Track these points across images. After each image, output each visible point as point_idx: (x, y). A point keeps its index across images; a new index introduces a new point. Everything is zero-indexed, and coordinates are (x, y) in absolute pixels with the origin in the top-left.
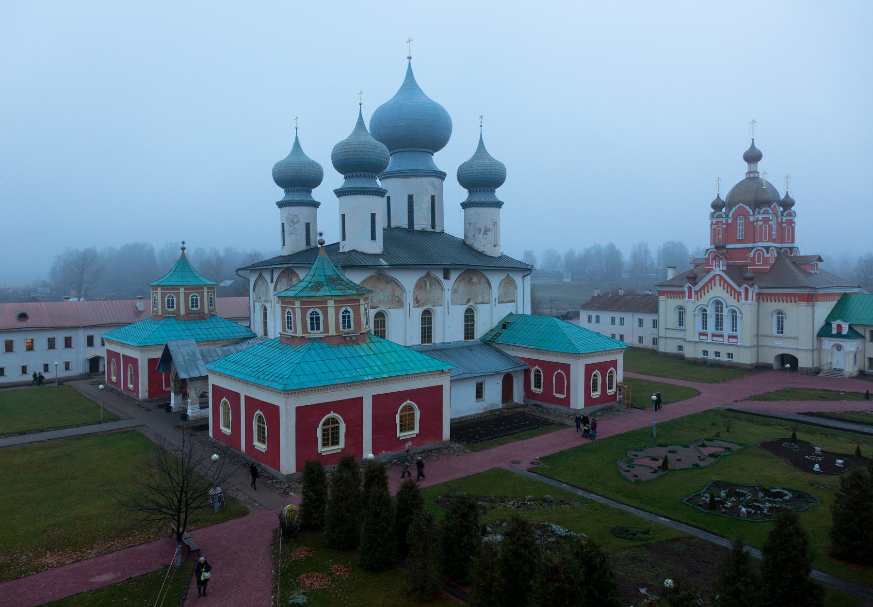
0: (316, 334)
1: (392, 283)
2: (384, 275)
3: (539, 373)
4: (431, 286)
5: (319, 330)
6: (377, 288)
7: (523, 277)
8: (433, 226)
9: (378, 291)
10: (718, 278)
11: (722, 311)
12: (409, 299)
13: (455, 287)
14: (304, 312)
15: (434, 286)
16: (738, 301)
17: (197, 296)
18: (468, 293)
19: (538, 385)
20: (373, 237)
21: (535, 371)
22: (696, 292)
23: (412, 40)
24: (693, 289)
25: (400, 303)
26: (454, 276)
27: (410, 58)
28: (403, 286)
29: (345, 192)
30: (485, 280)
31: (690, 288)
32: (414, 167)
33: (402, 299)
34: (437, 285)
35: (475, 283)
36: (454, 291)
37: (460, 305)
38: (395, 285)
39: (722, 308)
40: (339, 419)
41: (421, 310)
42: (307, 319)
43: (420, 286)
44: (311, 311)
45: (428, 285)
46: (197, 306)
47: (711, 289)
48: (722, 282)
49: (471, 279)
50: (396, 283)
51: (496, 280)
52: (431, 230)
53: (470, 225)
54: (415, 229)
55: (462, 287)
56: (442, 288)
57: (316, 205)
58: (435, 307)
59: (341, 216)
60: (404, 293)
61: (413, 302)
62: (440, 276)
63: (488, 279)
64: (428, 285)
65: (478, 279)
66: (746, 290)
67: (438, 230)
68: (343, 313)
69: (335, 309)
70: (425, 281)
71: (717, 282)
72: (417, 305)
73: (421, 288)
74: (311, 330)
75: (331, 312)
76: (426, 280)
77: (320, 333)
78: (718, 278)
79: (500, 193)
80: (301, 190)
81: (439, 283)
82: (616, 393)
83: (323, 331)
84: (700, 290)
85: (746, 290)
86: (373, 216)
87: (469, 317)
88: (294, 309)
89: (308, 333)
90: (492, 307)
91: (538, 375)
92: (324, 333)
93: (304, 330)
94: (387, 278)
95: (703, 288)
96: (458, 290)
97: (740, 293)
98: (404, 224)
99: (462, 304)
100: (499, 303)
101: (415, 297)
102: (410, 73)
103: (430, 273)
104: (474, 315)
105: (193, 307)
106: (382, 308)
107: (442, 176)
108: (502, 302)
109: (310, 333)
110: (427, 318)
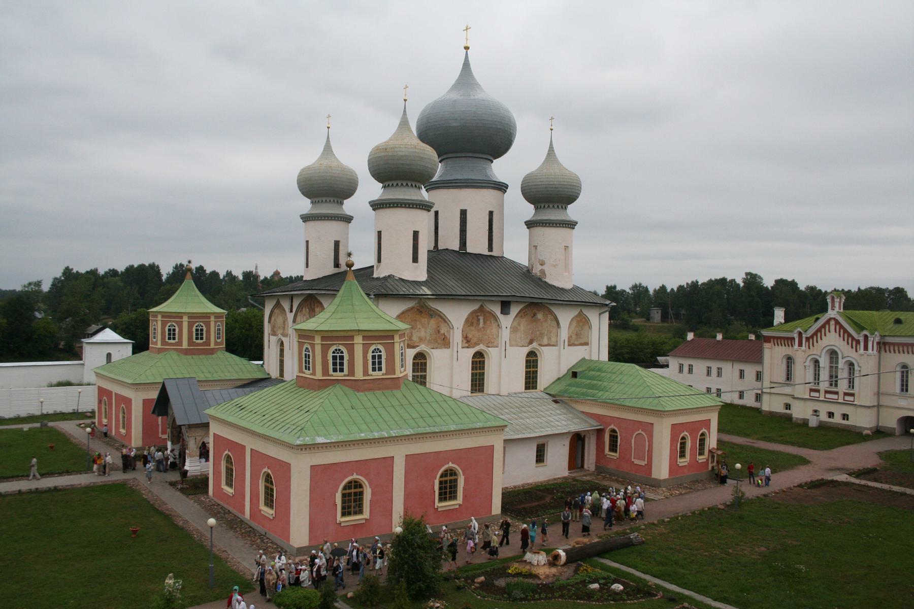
0: (338, 375)
1: (437, 317)
2: (427, 306)
3: (616, 434)
4: (485, 322)
5: (343, 371)
6: (418, 323)
7: (600, 314)
8: (490, 248)
9: (418, 327)
10: (832, 322)
11: (837, 362)
12: (457, 337)
13: (516, 324)
14: (325, 349)
15: (488, 322)
16: (856, 351)
17: (202, 327)
18: (531, 332)
19: (613, 448)
20: (415, 259)
21: (611, 431)
22: (808, 339)
23: (470, 28)
24: (803, 335)
25: (444, 342)
26: (515, 310)
27: (467, 48)
28: (450, 321)
29: (383, 204)
30: (552, 317)
31: (800, 334)
32: (466, 177)
33: (448, 336)
34: (492, 322)
35: (540, 319)
36: (514, 330)
37: (521, 347)
38: (440, 319)
39: (837, 358)
40: (366, 485)
41: (472, 351)
42: (328, 359)
43: (471, 321)
44: (333, 348)
45: (481, 321)
46: (202, 339)
47: (825, 335)
48: (838, 327)
49: (534, 315)
50: (440, 316)
51: (566, 317)
52: (486, 253)
53: (536, 248)
54: (468, 251)
55: (524, 324)
56: (499, 325)
57: (348, 219)
58: (489, 348)
59: (377, 233)
60: (451, 330)
61: (462, 341)
62: (497, 310)
63: (555, 314)
64: (481, 321)
65: (543, 315)
66: (866, 337)
67: (495, 253)
68: (373, 352)
69: (322, 348)
70: (478, 316)
71: (832, 327)
72: (467, 345)
73: (472, 324)
74: (333, 371)
75: (358, 351)
76: (479, 314)
77: (344, 376)
78: (832, 322)
79: (573, 211)
80: (330, 201)
81: (496, 319)
82: (708, 460)
83: (347, 374)
84: (812, 337)
85: (866, 337)
86: (416, 234)
87: (532, 361)
88: (313, 346)
89: (329, 375)
90: (559, 351)
91: (614, 435)
92: (348, 376)
94: (431, 310)
95: (815, 334)
96: (519, 328)
97: (858, 342)
98: (455, 246)
99: (523, 346)
100: (569, 345)
101: (465, 336)
102: (466, 65)
103: (485, 306)
104: (537, 360)
105: (197, 339)
106: (423, 347)
107: (502, 187)
108: (574, 345)
109: (332, 376)
110: (479, 361)
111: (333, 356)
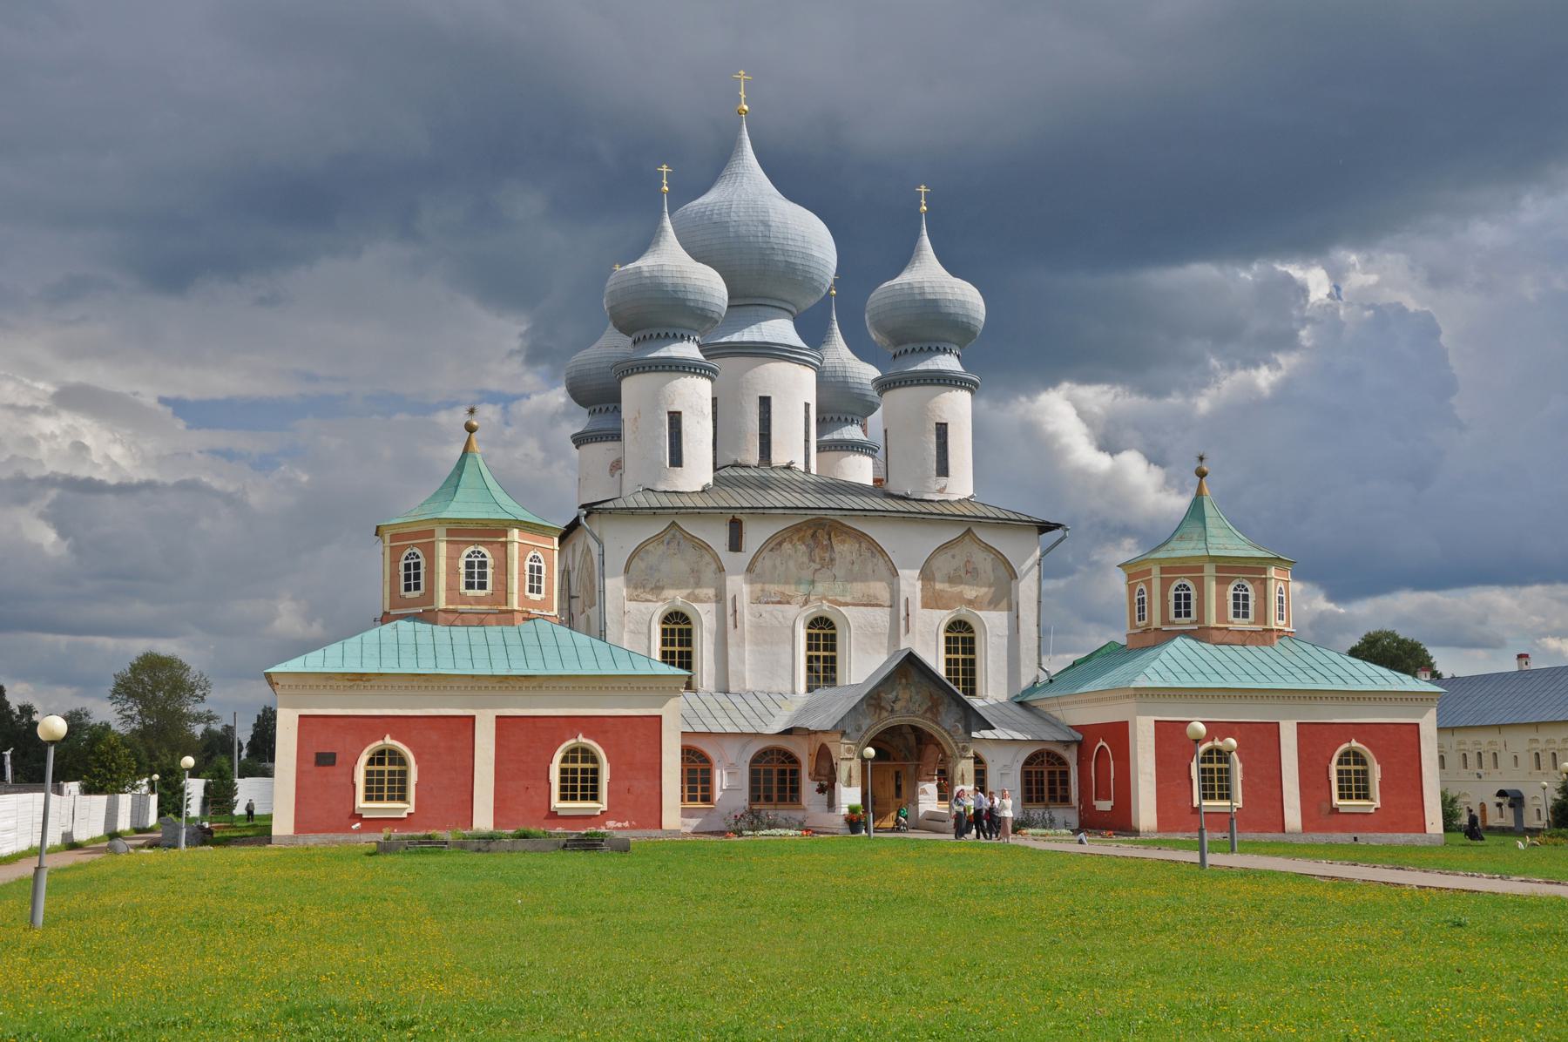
0: (1240, 624)
5: (1248, 617)
74: (1234, 617)
77: (1250, 623)
89: (1228, 622)
92: (1254, 623)
93: (1221, 615)
105: (531, 590)
109: (1232, 623)
111: (1234, 595)
